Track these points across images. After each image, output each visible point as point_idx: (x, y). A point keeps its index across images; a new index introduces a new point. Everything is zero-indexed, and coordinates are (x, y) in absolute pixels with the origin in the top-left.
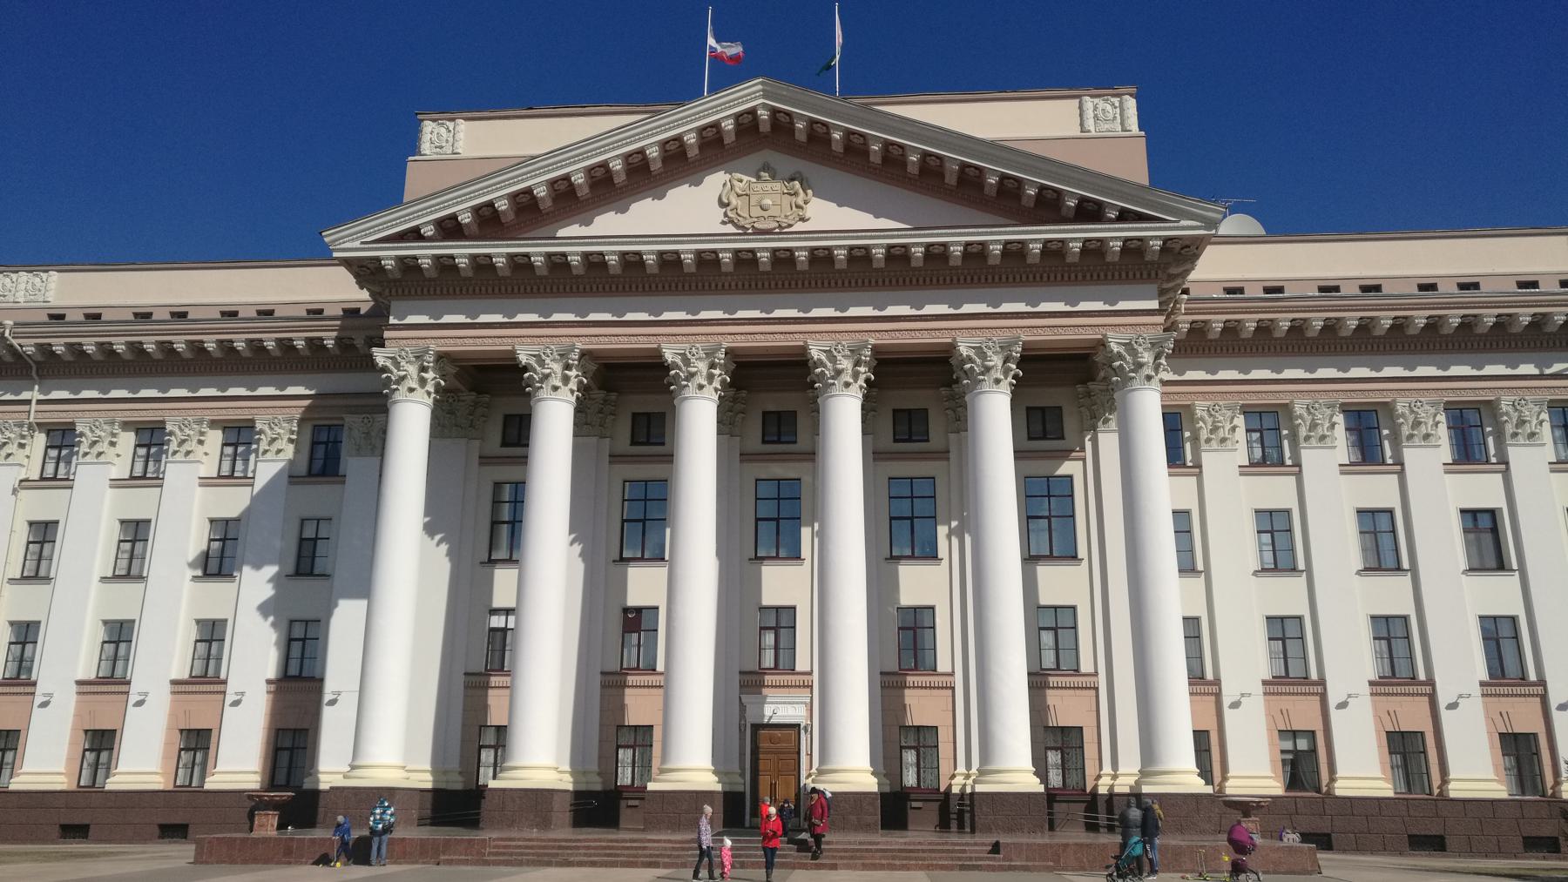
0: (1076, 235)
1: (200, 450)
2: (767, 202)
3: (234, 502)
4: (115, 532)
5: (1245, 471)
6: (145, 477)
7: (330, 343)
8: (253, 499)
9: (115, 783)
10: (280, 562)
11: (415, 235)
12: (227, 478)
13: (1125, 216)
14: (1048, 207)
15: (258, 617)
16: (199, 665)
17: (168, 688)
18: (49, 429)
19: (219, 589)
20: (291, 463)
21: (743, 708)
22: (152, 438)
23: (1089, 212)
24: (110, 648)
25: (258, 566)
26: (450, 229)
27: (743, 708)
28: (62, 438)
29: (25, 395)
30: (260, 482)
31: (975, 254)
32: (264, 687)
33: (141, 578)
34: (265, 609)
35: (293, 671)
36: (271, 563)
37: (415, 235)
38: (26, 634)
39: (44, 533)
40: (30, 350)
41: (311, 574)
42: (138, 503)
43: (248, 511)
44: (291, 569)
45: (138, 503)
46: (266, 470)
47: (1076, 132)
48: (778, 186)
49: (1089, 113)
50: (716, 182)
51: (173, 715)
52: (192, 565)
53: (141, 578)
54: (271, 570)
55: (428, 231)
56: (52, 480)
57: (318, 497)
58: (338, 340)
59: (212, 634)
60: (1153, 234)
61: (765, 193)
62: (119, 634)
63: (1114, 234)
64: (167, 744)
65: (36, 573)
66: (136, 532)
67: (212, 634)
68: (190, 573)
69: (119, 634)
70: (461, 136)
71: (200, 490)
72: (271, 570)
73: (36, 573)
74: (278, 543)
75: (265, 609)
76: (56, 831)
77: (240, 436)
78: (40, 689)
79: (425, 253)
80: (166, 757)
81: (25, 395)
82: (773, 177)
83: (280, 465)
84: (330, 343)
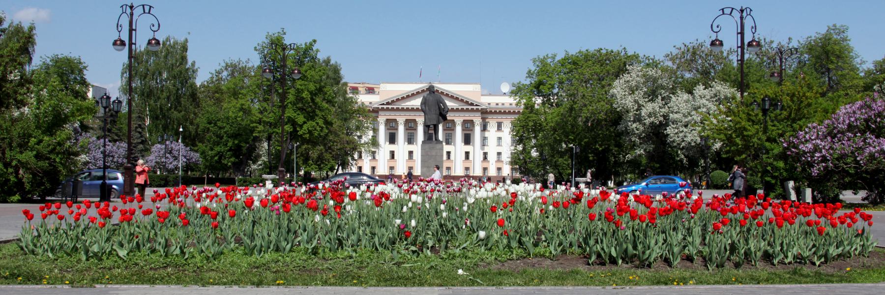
0: (470, 107)
5: (496, 131)
11: (383, 104)
13: (476, 105)
26: (388, 103)
37: (383, 104)
60: (480, 108)
63: (475, 108)
79: (385, 107)
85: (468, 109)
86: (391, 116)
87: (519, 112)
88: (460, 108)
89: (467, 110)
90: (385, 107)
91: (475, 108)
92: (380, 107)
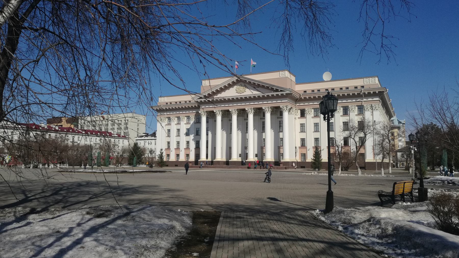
0: (275, 94)
1: (184, 120)
2: (241, 90)
3: (189, 126)
4: (176, 130)
5: (312, 117)
6: (179, 124)
7: (197, 106)
8: (191, 126)
9: (180, 160)
10: (194, 134)
12: (188, 123)
13: (281, 91)
14: (272, 89)
15: (192, 141)
16: (187, 146)
17: (184, 149)
18: (168, 118)
19: (188, 137)
20: (194, 121)
21: (245, 151)
22: (179, 118)
23: (277, 91)
24: (177, 144)
25: (192, 135)
26: (205, 97)
27: (245, 151)
28: (169, 119)
29: (165, 114)
30: (191, 124)
31: (263, 96)
32: (194, 149)
33: (180, 136)
34: (193, 140)
35: (197, 147)
36: (193, 134)
37: (201, 98)
38: (169, 143)
39: (169, 131)
40: (165, 109)
41: (198, 135)
42: (178, 127)
43: (190, 127)
44: (196, 134)
45: (178, 127)
46: (192, 122)
47: (279, 77)
48: (242, 87)
49: (281, 74)
50: (235, 87)
51: (185, 153)
52: (185, 134)
53: (180, 136)
54: (193, 135)
55: (203, 97)
56: (169, 124)
57: (197, 125)
58: (198, 106)
59: (188, 142)
60: (284, 93)
61: (241, 88)
62: (178, 143)
63: (280, 93)
64: (185, 156)
65: (169, 136)
66: (179, 130)
67: (188, 142)
68: (185, 136)
69: (178, 143)
70: (207, 82)
71: (185, 125)
72: (193, 135)
73: (169, 136)
74: (194, 131)
75: (193, 140)
76: (174, 166)
77: (188, 117)
78: (171, 149)
79: (203, 100)
80: (185, 157)
81: (165, 114)
82: (242, 86)
83: (193, 122)
84: (197, 106)
85: (273, 95)
86: (210, 108)
87: (319, 97)
88: (266, 95)
89: (273, 97)
90: (203, 100)
91: (280, 93)
92: (199, 100)
